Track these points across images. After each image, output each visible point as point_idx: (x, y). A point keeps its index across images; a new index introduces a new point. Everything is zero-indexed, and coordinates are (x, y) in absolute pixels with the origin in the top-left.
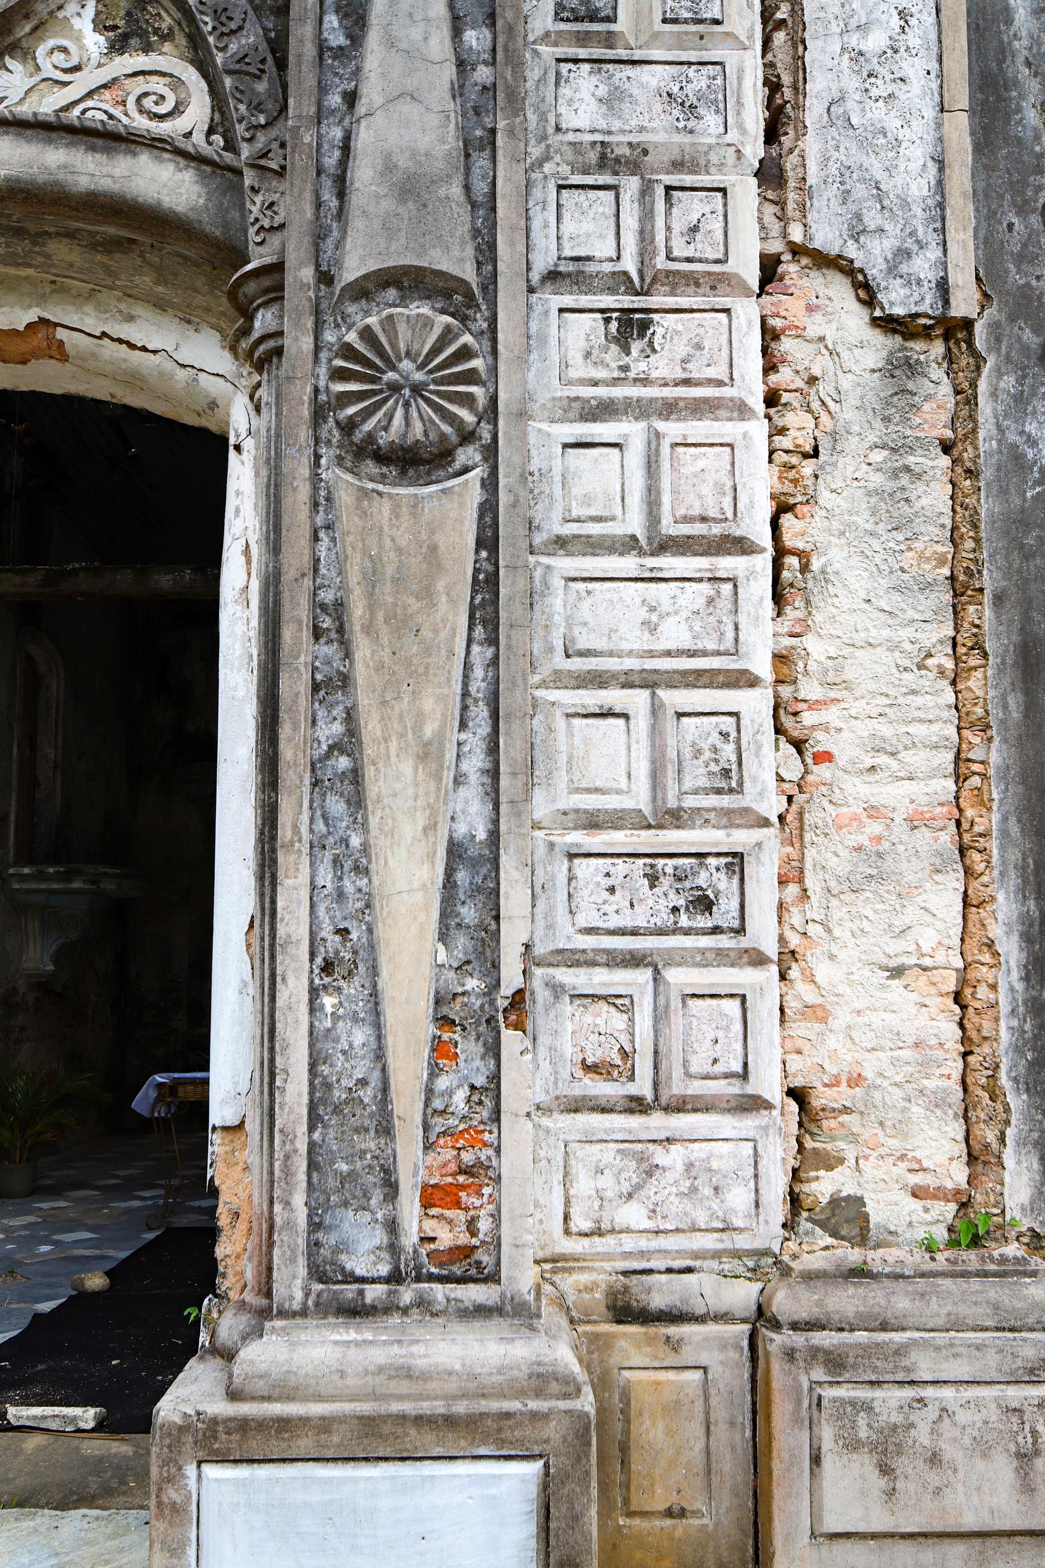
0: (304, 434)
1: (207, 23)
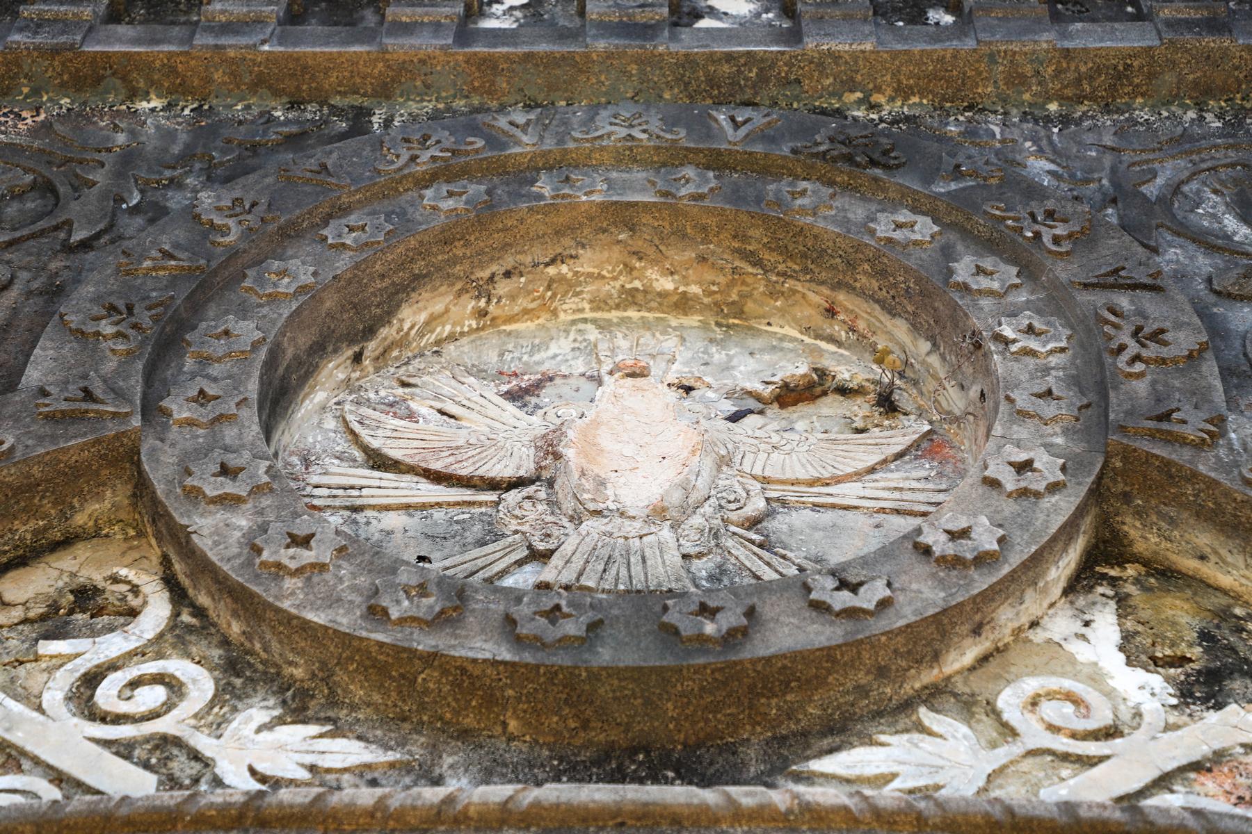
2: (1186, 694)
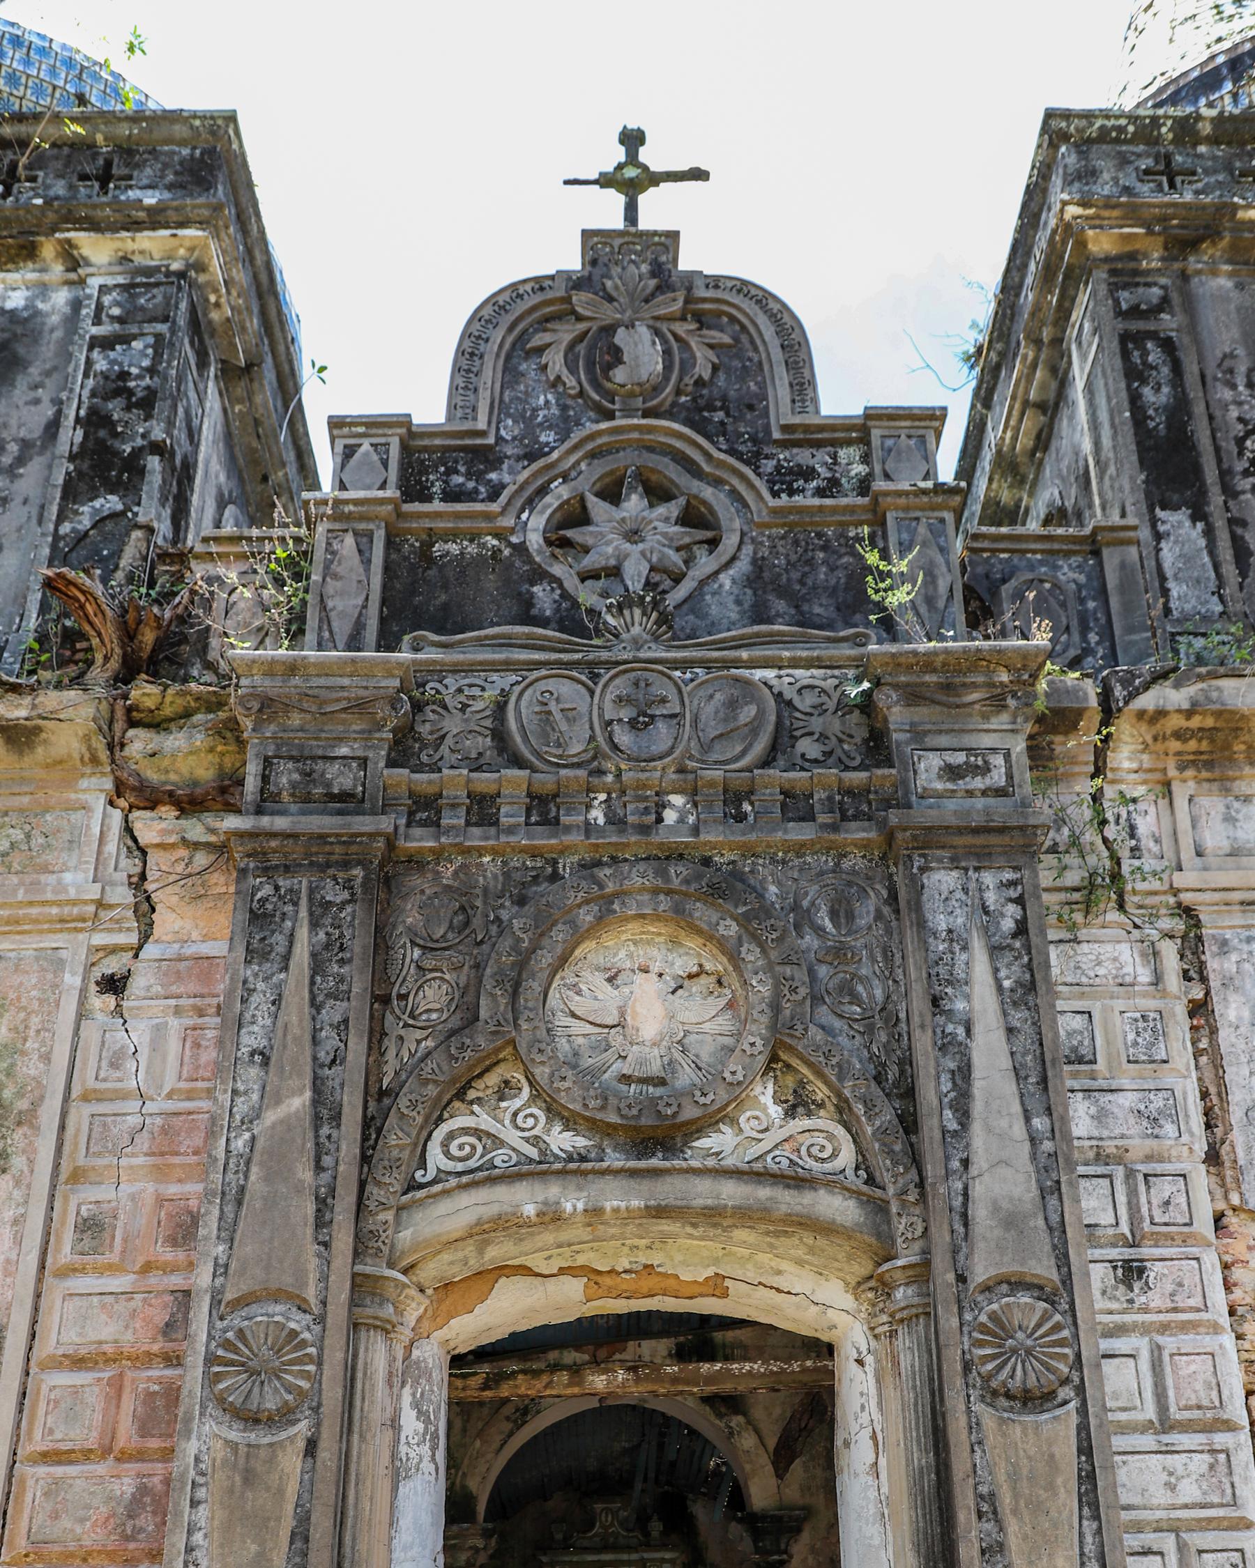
0: (959, 1382)
1: (859, 1109)
2: (786, 1114)
